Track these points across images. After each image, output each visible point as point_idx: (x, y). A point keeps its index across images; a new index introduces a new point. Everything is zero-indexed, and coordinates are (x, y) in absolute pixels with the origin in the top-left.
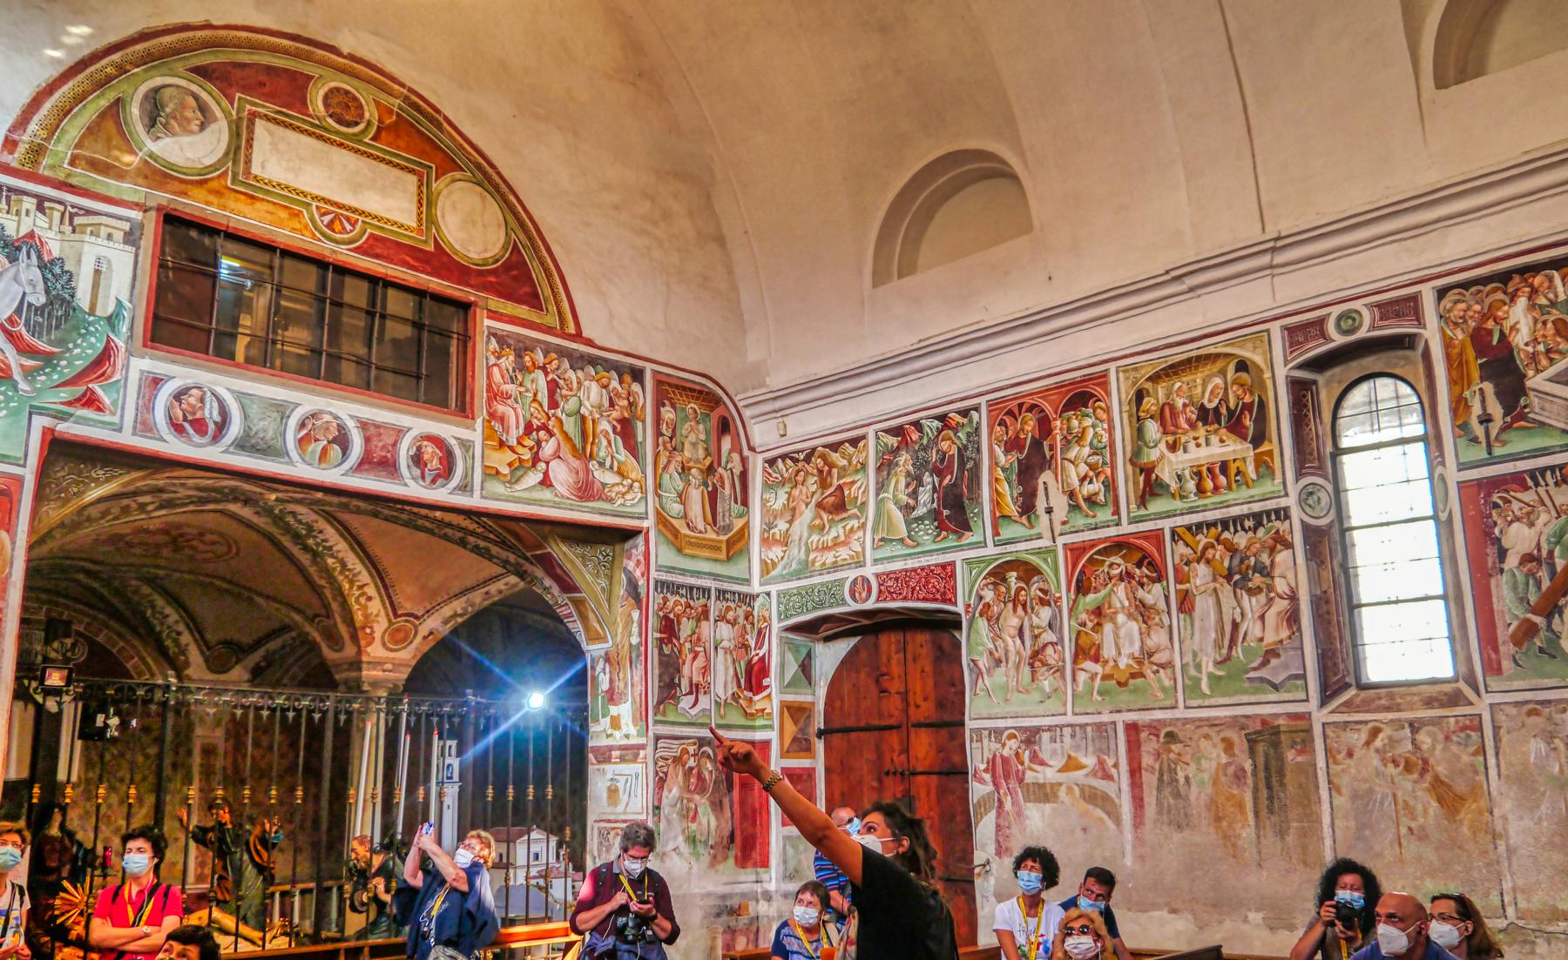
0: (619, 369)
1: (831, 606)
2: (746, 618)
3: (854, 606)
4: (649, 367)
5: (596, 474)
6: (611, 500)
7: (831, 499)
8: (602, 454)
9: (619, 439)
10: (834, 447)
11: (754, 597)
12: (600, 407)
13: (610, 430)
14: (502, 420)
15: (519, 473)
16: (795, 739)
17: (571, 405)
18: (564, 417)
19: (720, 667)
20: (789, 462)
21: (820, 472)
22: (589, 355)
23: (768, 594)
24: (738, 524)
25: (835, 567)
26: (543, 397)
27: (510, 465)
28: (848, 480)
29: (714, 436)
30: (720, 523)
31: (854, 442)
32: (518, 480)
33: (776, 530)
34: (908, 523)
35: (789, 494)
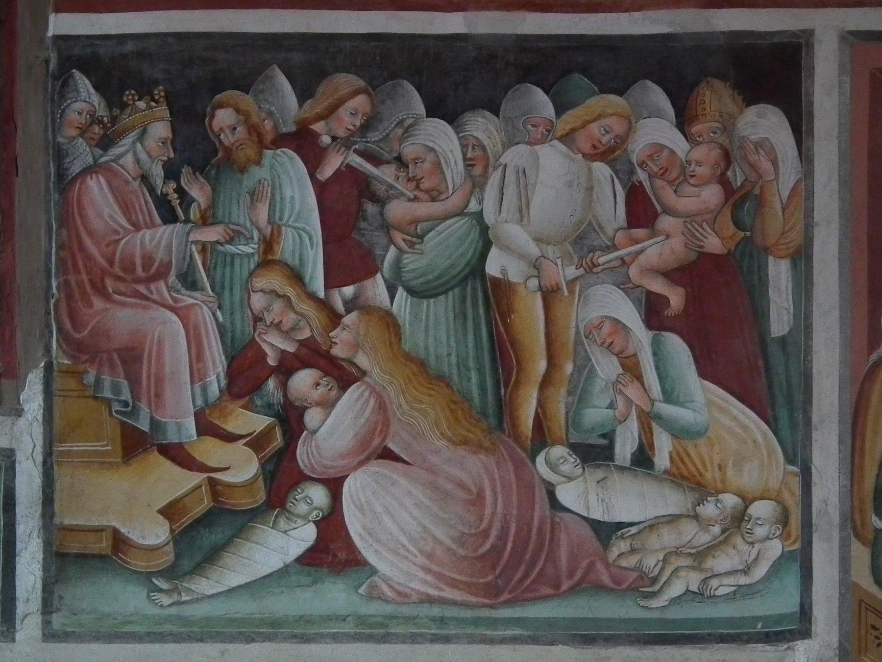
0: (676, 69)
4: (827, 28)
5: (567, 495)
6: (643, 585)
8: (596, 414)
9: (677, 347)
12: (583, 241)
13: (630, 316)
14: (131, 358)
15: (210, 538)
17: (441, 249)
22: (525, 43)
26: (305, 241)
27: (169, 512)
32: (211, 557)
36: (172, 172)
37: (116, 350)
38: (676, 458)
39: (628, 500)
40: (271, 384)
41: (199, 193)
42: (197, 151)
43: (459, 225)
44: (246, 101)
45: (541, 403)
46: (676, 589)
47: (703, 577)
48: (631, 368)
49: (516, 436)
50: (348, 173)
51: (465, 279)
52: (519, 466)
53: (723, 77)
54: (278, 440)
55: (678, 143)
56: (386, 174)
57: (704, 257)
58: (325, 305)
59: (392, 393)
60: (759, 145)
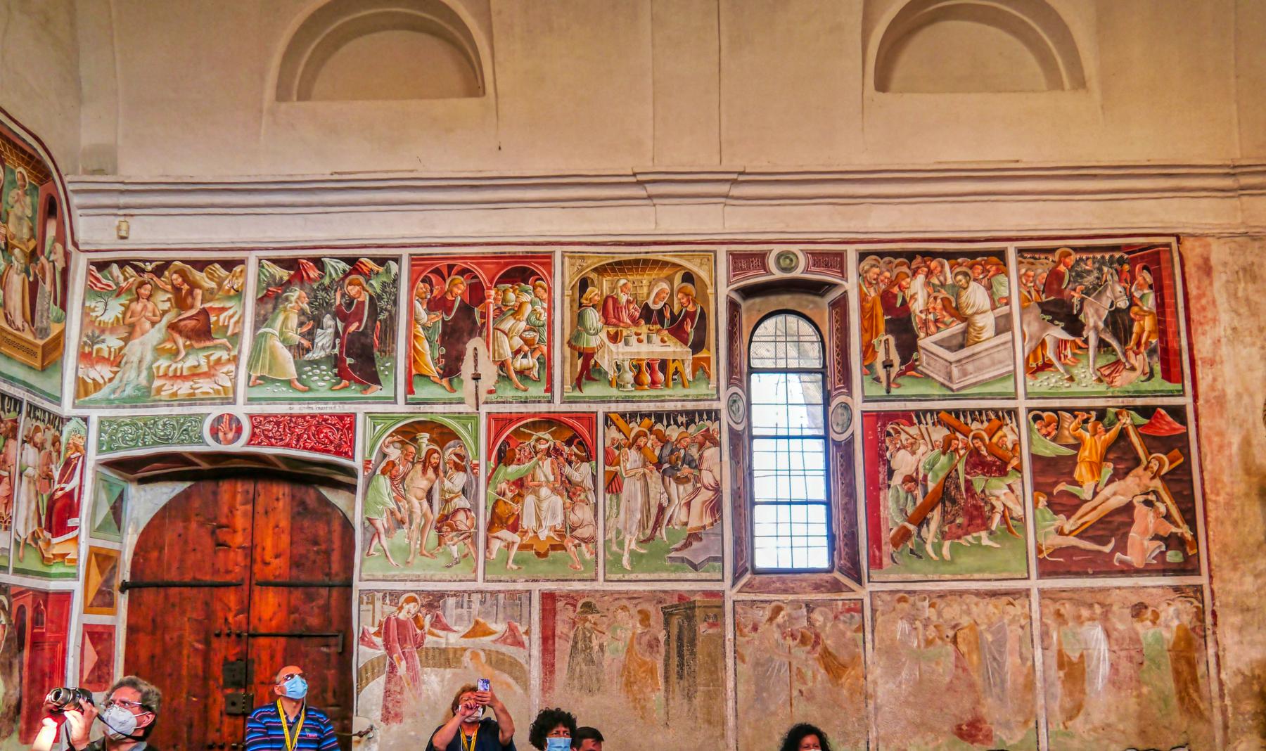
1: (182, 443)
2: (53, 444)
3: (213, 446)
7: (191, 323)
10: (201, 265)
11: (64, 420)
16: (99, 592)
19: (23, 499)
20: (129, 270)
21: (177, 290)
23: (85, 420)
24: (55, 330)
25: (191, 399)
28: (217, 305)
29: (38, 222)
30: (38, 324)
31: (228, 265)
33: (103, 346)
34: (299, 366)
35: (127, 308)
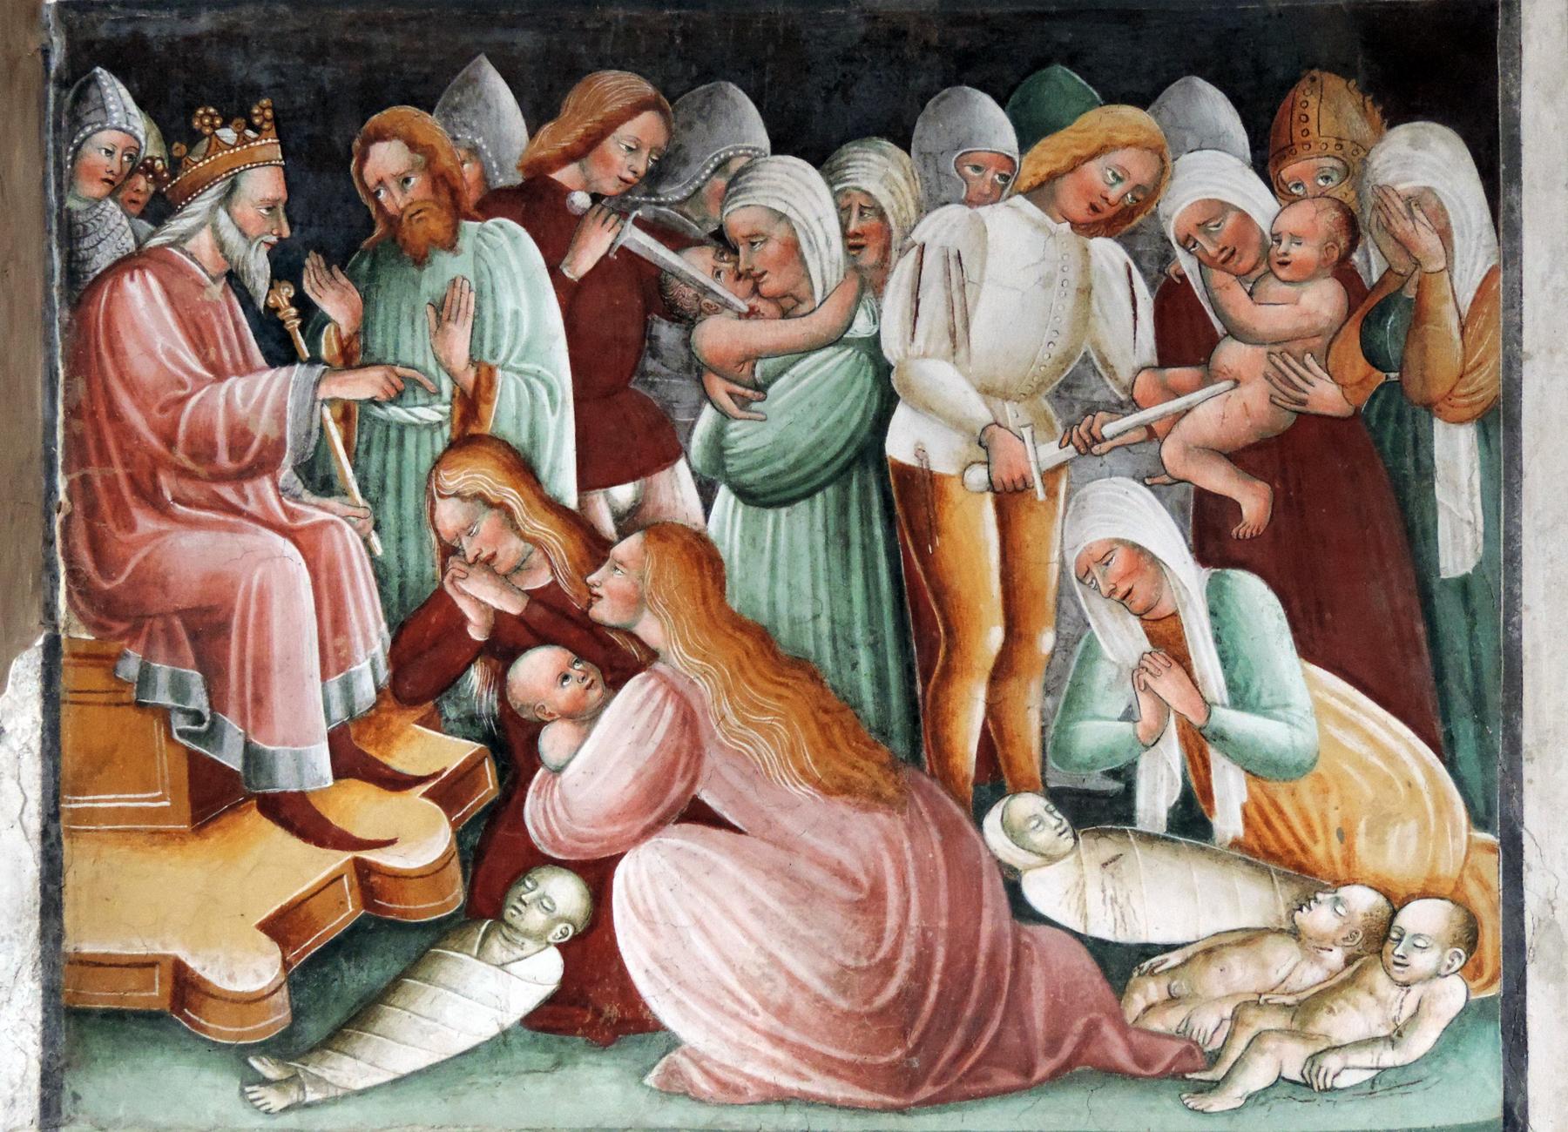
5: (1041, 891)
9: (1254, 595)
12: (1074, 393)
13: (1168, 540)
14: (208, 629)
15: (358, 978)
17: (804, 407)
18: (726, 521)
26: (541, 400)
27: (282, 927)
32: (362, 1014)
36: (285, 267)
37: (178, 612)
38: (1257, 816)
39: (1165, 900)
40: (476, 677)
41: (337, 304)
42: (335, 227)
43: (833, 364)
44: (429, 125)
45: (994, 712)
46: (1258, 1075)
47: (1311, 1050)
48: (1168, 641)
49: (946, 775)
50: (623, 262)
51: (846, 469)
52: (951, 834)
53: (1344, 70)
54: (490, 785)
55: (1257, 200)
56: (695, 265)
57: (1307, 421)
58: (577, 522)
59: (706, 691)
60: (1413, 202)
